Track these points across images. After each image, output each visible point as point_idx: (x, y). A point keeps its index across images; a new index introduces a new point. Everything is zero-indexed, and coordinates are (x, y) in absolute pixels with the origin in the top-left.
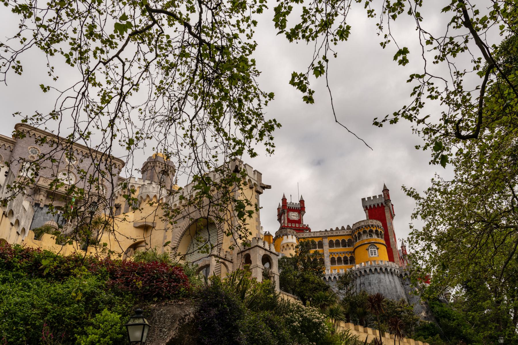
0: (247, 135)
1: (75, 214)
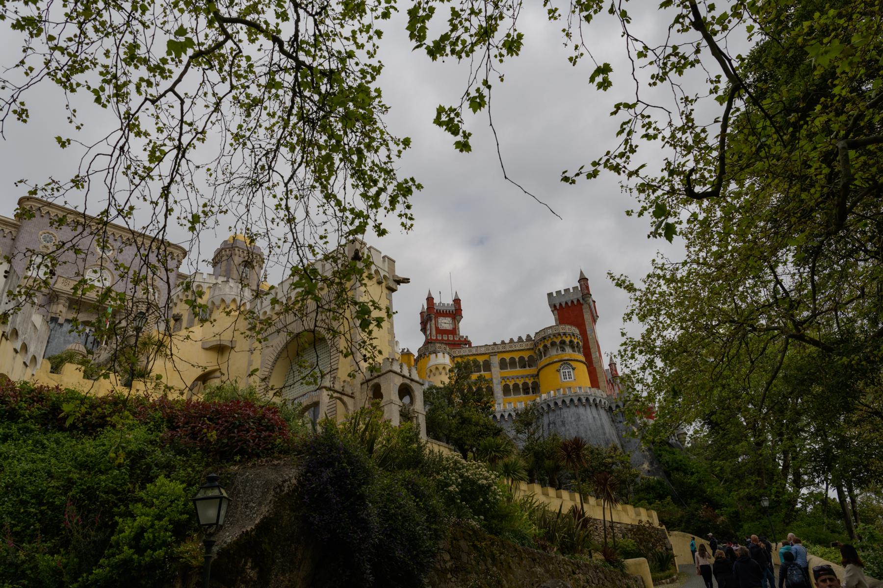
0: (371, 203)
1: (113, 331)
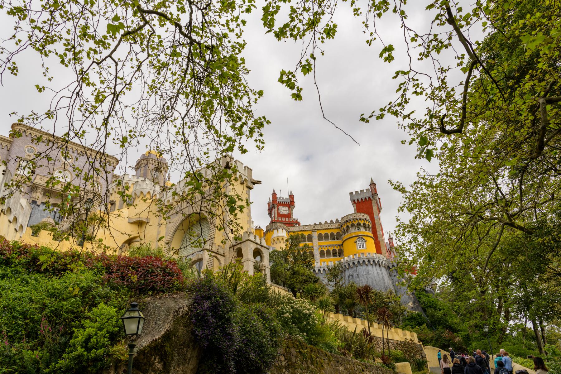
0: (237, 132)
1: (72, 210)
